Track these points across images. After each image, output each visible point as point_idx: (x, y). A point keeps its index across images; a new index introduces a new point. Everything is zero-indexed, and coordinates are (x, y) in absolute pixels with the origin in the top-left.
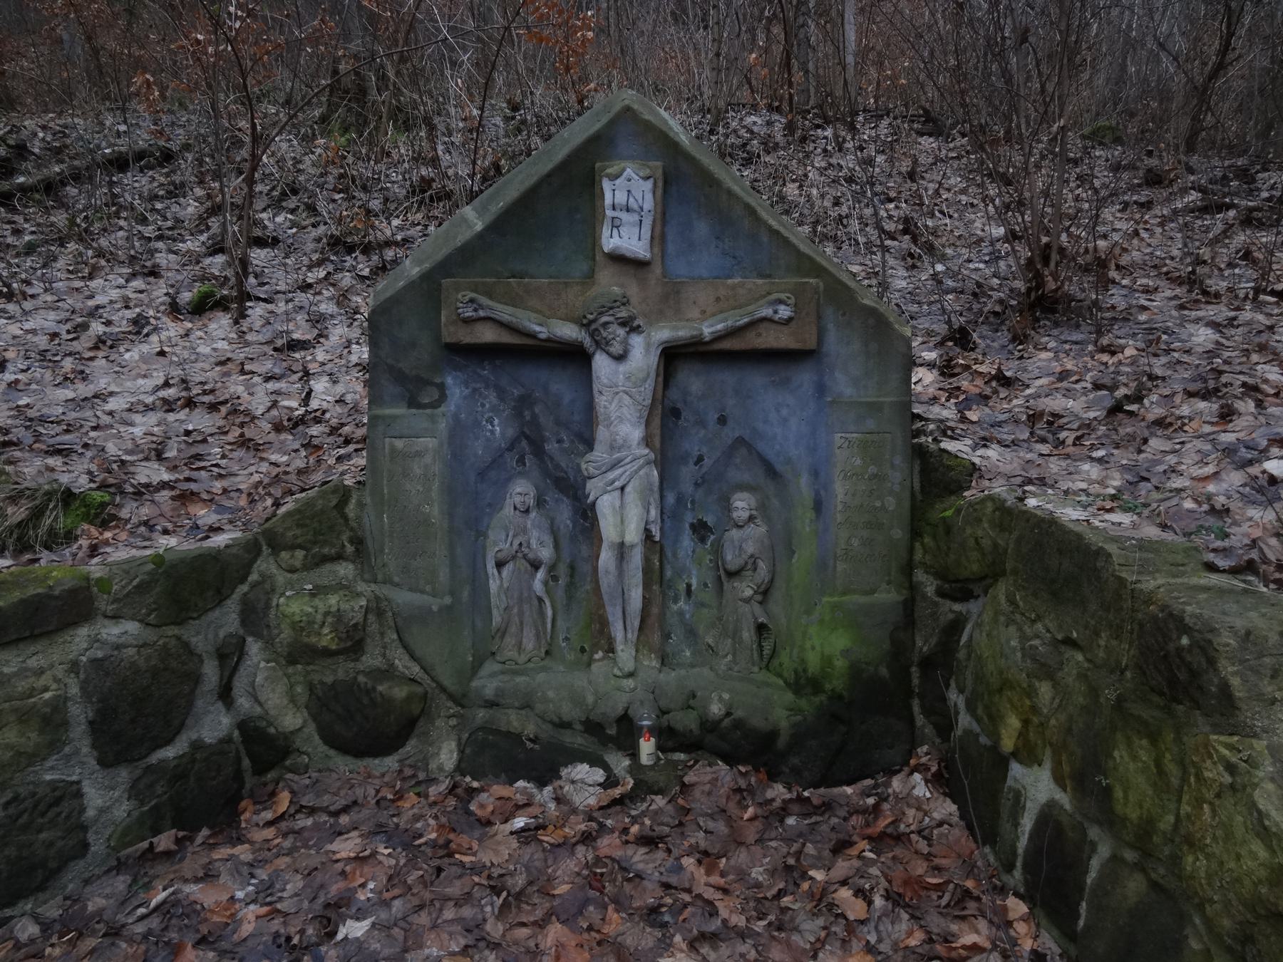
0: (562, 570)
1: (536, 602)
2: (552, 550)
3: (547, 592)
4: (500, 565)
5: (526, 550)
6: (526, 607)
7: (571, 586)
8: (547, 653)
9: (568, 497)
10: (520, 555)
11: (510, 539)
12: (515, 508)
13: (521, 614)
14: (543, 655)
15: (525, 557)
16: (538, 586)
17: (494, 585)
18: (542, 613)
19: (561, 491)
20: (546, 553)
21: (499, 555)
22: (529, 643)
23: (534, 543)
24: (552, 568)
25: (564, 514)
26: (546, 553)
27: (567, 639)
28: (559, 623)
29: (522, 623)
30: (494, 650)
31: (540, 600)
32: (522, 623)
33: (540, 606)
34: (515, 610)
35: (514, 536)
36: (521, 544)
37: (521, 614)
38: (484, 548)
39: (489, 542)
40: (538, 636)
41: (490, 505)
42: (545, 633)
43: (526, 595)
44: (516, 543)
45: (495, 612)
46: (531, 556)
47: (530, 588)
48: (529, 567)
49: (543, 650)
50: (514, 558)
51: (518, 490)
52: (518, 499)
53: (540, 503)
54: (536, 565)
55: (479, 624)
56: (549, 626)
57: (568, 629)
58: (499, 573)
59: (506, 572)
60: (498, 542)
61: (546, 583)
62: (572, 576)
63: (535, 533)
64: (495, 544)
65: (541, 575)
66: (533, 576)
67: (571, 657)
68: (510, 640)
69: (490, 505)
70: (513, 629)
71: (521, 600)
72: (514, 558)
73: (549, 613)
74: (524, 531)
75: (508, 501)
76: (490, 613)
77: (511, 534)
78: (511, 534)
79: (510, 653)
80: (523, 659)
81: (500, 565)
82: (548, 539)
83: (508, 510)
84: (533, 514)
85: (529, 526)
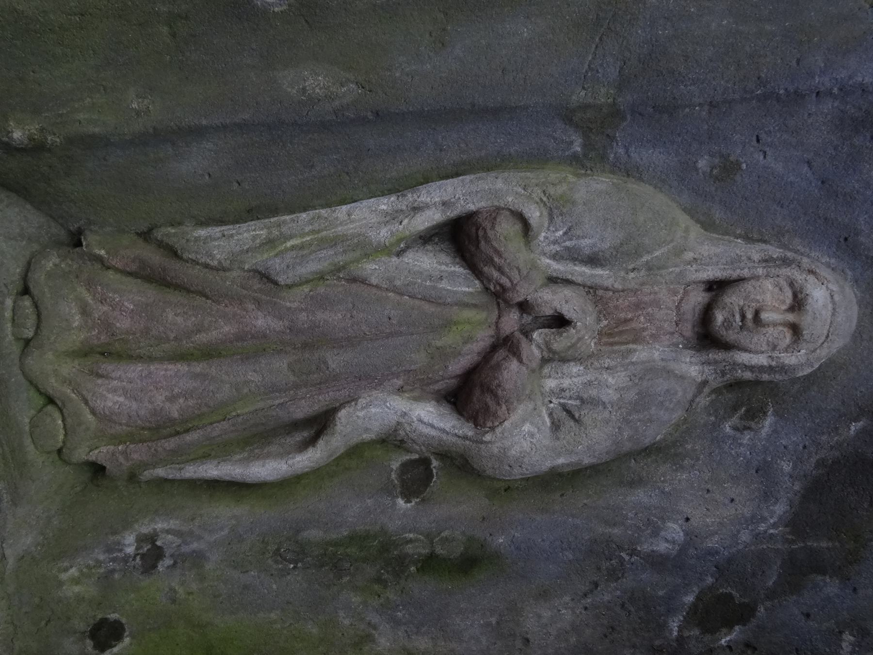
0: (454, 513)
1: (304, 408)
2: (547, 465)
3: (356, 451)
4: (460, 236)
5: (532, 351)
6: (280, 367)
7: (383, 560)
8: (97, 470)
9: (797, 524)
10: (511, 321)
11: (581, 272)
12: (717, 287)
13: (250, 347)
14: (81, 454)
15: (505, 345)
16: (377, 411)
17: (367, 217)
18: (260, 437)
19: (816, 490)
20: (525, 437)
21: (507, 228)
22: (123, 393)
23: (571, 378)
24: (460, 464)
25: (712, 510)
26: (525, 437)
27: (152, 555)
28: (225, 513)
29: (209, 353)
30: (95, 244)
31: (319, 424)
32: (209, 353)
33: (296, 425)
34: (261, 321)
35: (592, 290)
36: (560, 322)
37: (250, 347)
38: (537, 159)
39: (560, 180)
40: (160, 428)
41: (728, 169)
42: (179, 456)
43: (335, 361)
44: (554, 300)
45: (249, 233)
46: (512, 372)
47: (372, 379)
48: (457, 366)
49: (101, 454)
50: (499, 296)
51: (818, 295)
52: (769, 295)
53: (746, 396)
54: (470, 394)
55: (195, 163)
56: (212, 470)
57: (198, 558)
58: (426, 238)
59: (433, 265)
60: (566, 220)
61: (392, 440)
62: (430, 564)
63: (612, 384)
64: (555, 208)
65: (430, 419)
66: (418, 385)
67: (74, 581)
68: (127, 304)
69: (728, 169)
70: (176, 316)
71: (310, 341)
72: (499, 296)
73: (266, 469)
74: (618, 334)
75: (756, 252)
76: (252, 213)
77: (602, 275)
78: (602, 275)
79: (72, 314)
80: (54, 368)
81: (460, 236)
82: (593, 441)
83: (710, 254)
84: (692, 367)
85: (641, 354)
